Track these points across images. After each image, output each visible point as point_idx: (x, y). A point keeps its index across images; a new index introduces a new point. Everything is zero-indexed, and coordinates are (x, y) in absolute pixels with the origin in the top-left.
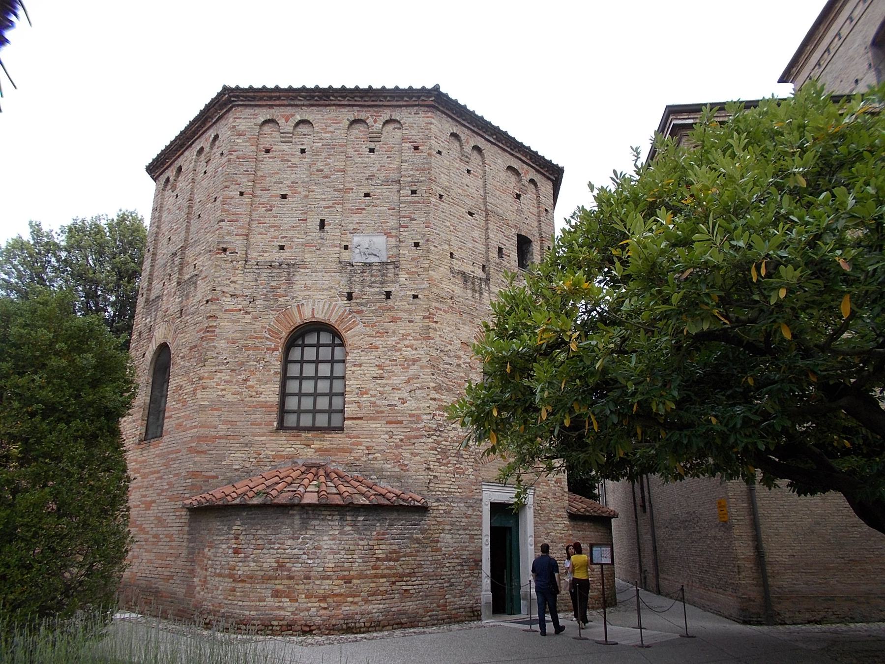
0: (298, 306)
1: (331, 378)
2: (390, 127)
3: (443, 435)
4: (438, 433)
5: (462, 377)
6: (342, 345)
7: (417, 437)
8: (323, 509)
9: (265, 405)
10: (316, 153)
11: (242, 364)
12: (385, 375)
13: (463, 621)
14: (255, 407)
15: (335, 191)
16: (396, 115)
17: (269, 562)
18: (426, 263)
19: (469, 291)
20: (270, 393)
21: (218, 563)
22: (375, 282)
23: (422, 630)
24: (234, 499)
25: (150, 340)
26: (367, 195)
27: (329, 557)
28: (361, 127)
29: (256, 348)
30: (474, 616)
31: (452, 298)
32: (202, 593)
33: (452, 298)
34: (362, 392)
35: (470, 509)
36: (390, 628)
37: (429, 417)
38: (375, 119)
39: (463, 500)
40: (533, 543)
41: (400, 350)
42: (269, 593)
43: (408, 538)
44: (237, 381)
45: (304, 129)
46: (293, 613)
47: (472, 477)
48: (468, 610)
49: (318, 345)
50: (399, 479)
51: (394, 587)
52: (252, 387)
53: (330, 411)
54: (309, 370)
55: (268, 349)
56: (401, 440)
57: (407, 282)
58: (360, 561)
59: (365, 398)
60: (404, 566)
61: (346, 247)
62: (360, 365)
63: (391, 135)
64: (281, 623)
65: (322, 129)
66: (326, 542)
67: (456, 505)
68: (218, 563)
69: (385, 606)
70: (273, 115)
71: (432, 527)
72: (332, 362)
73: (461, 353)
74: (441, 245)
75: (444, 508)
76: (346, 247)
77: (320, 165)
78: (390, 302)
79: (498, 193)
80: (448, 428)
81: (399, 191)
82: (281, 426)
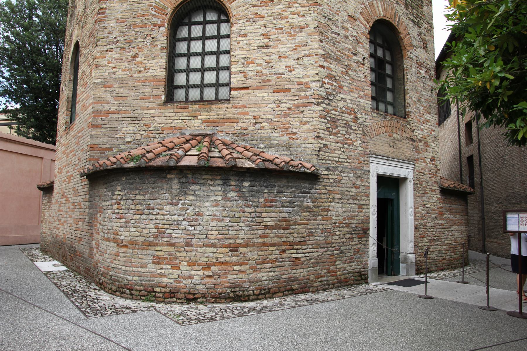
1: (218, 53)
3: (333, 104)
4: (327, 102)
5: (350, 49)
6: (228, 21)
7: (305, 105)
8: (204, 172)
9: (153, 80)
11: (131, 41)
12: (271, 43)
13: (352, 285)
14: (144, 82)
17: (150, 227)
20: (158, 68)
21: (105, 227)
23: (313, 296)
27: (212, 224)
29: (144, 25)
30: (362, 279)
32: (97, 255)
34: (247, 61)
35: (359, 179)
36: (281, 294)
37: (318, 84)
39: (353, 170)
40: (412, 213)
41: (286, 18)
42: (150, 259)
43: (298, 206)
44: (127, 58)
46: (175, 281)
47: (360, 148)
48: (356, 274)
49: (204, 23)
50: (287, 147)
51: (284, 255)
52: (141, 63)
53: (217, 85)
54: (196, 46)
55: (155, 25)
56: (289, 109)
58: (247, 228)
59: (251, 67)
60: (295, 235)
62: (245, 35)
64: (163, 290)
66: (208, 209)
67: (345, 175)
68: (105, 227)
69: (275, 274)
71: (322, 196)
75: (334, 177)
80: (337, 98)
82: (170, 98)
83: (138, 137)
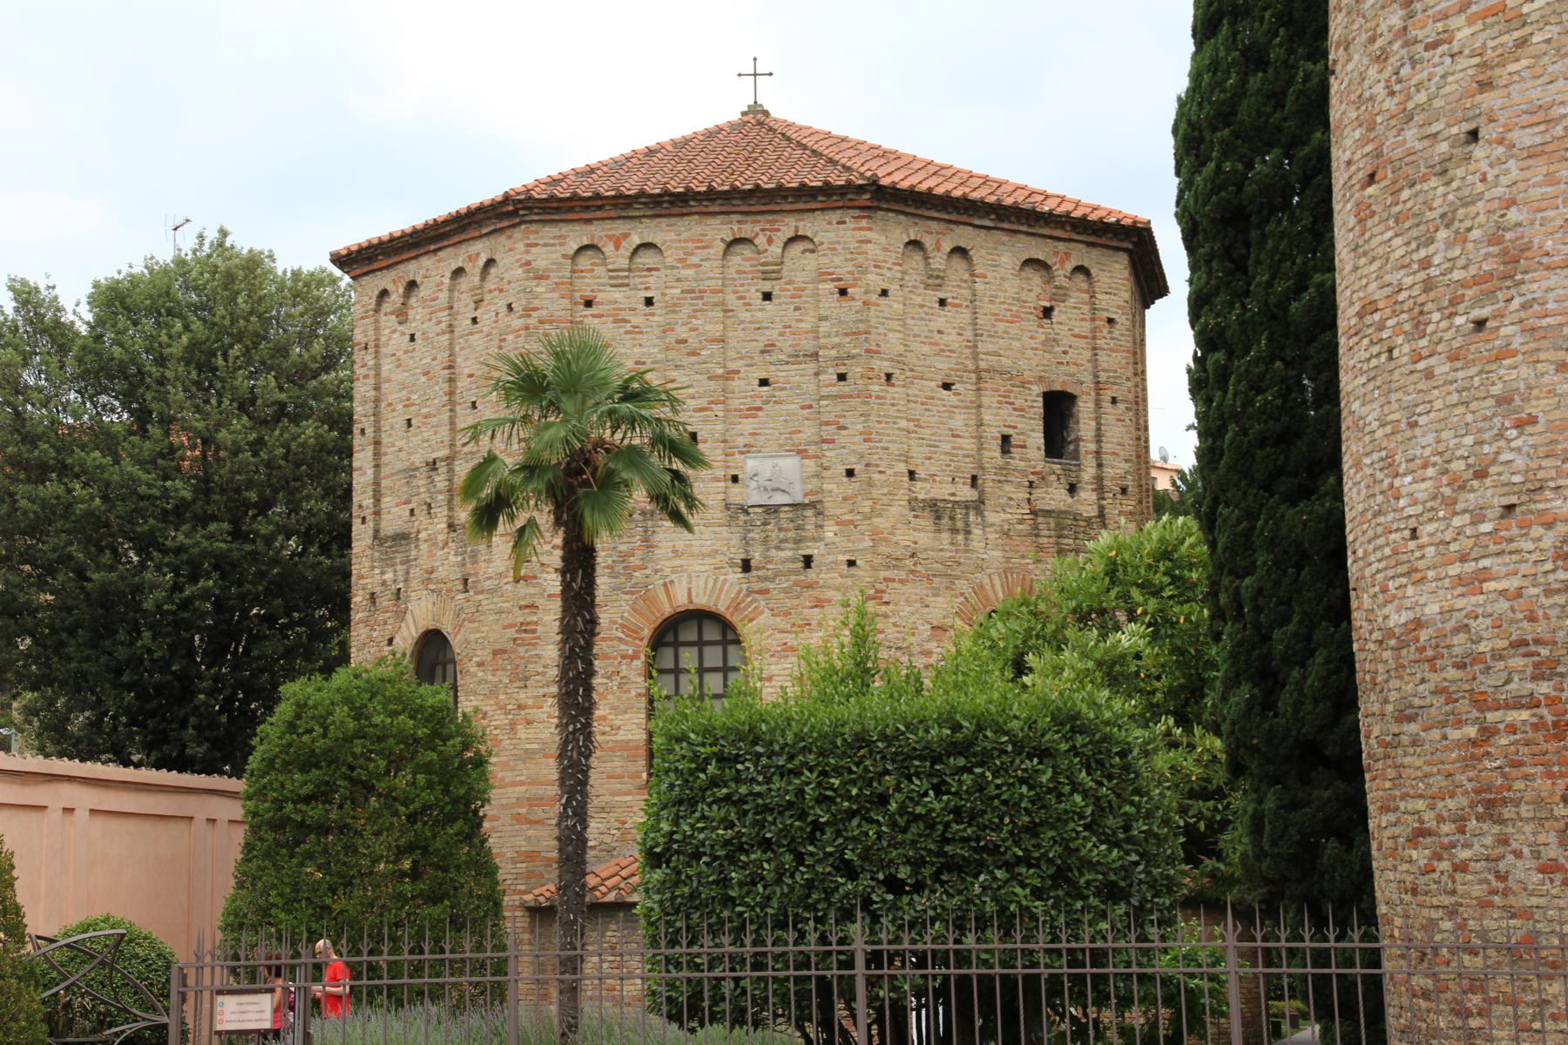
0: (665, 585)
2: (798, 247)
6: (738, 642)
9: (625, 746)
10: (672, 308)
15: (710, 378)
16: (807, 225)
18: (866, 506)
19: (946, 536)
22: (785, 541)
24: (604, 894)
25: (401, 615)
26: (764, 382)
28: (746, 250)
31: (913, 556)
33: (913, 556)
38: (770, 235)
45: (647, 259)
49: (700, 644)
55: (624, 657)
57: (837, 539)
61: (735, 479)
63: (800, 265)
65: (680, 260)
70: (593, 236)
72: (726, 670)
73: (932, 645)
74: (890, 466)
76: (735, 479)
77: (681, 332)
78: (811, 575)
79: (1001, 326)
81: (817, 374)
83: (608, 839)
